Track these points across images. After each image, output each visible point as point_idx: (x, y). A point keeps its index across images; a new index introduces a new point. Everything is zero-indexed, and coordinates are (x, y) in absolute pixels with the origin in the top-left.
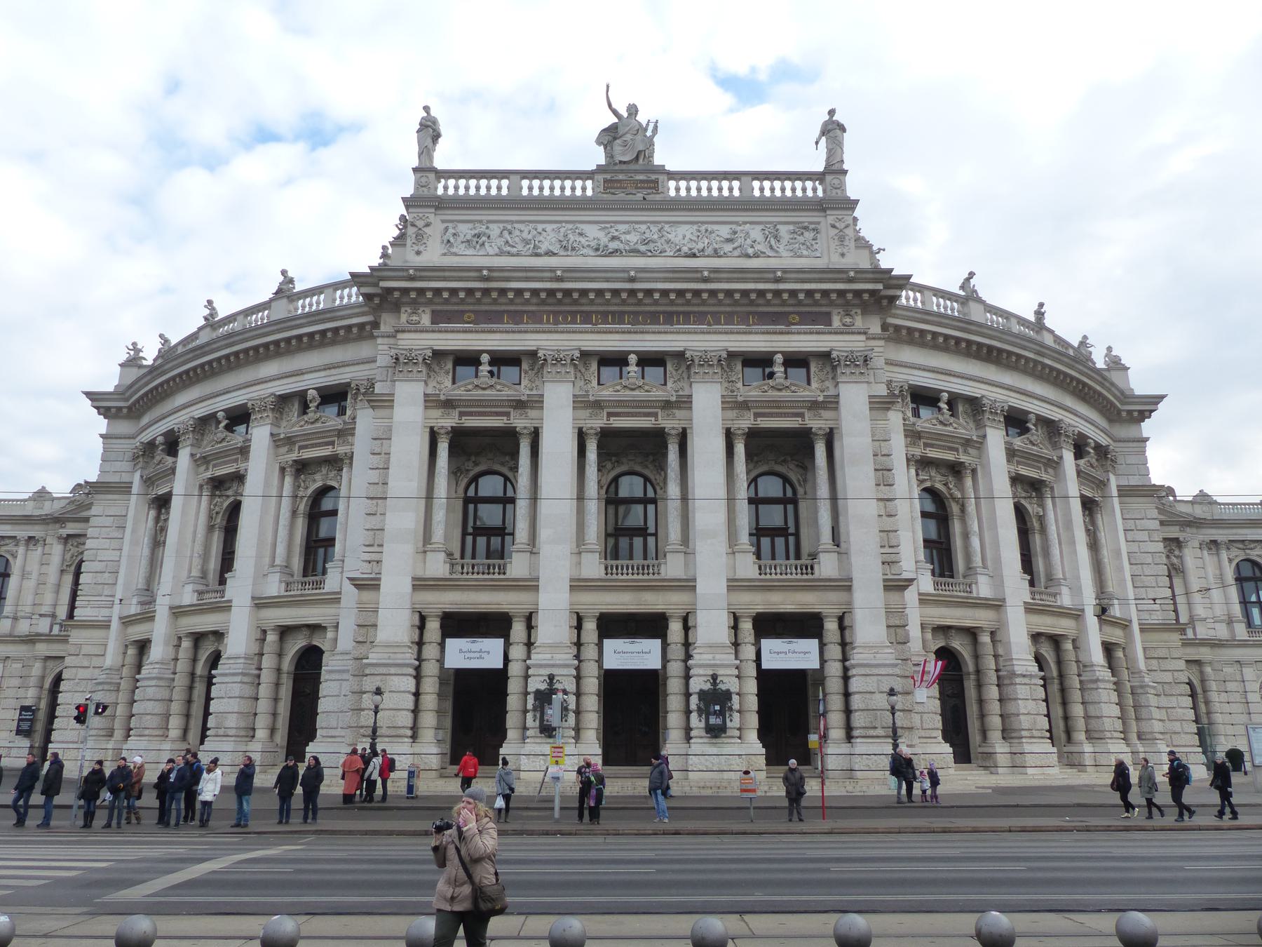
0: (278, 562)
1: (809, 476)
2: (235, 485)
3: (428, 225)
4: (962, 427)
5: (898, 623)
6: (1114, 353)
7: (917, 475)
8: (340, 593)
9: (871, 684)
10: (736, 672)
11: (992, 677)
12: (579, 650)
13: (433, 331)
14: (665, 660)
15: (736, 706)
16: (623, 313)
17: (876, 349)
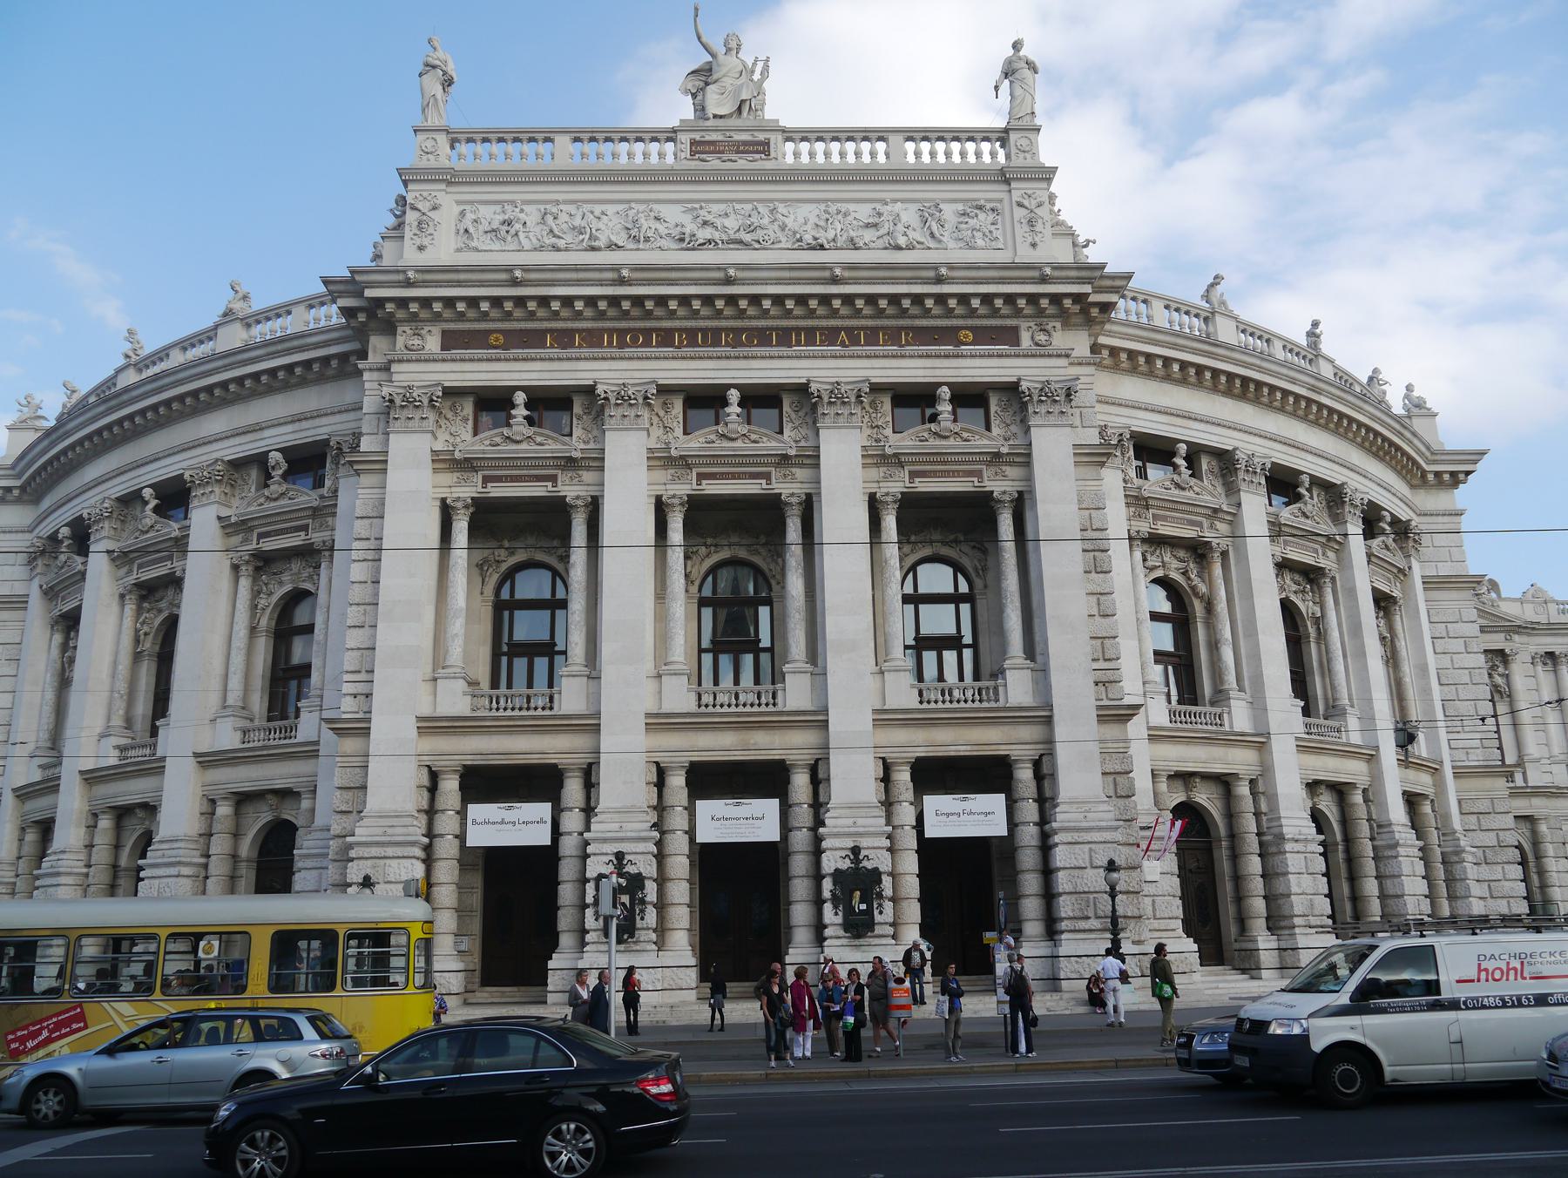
0: (230, 701)
1: (990, 563)
2: (170, 592)
3: (434, 208)
4: (1208, 492)
5: (1118, 768)
6: (1416, 394)
7: (1145, 560)
8: (317, 743)
9: (1080, 855)
10: (887, 843)
11: (1252, 843)
12: (660, 817)
13: (444, 360)
14: (786, 827)
15: (888, 892)
16: (717, 332)
17: (1083, 379)
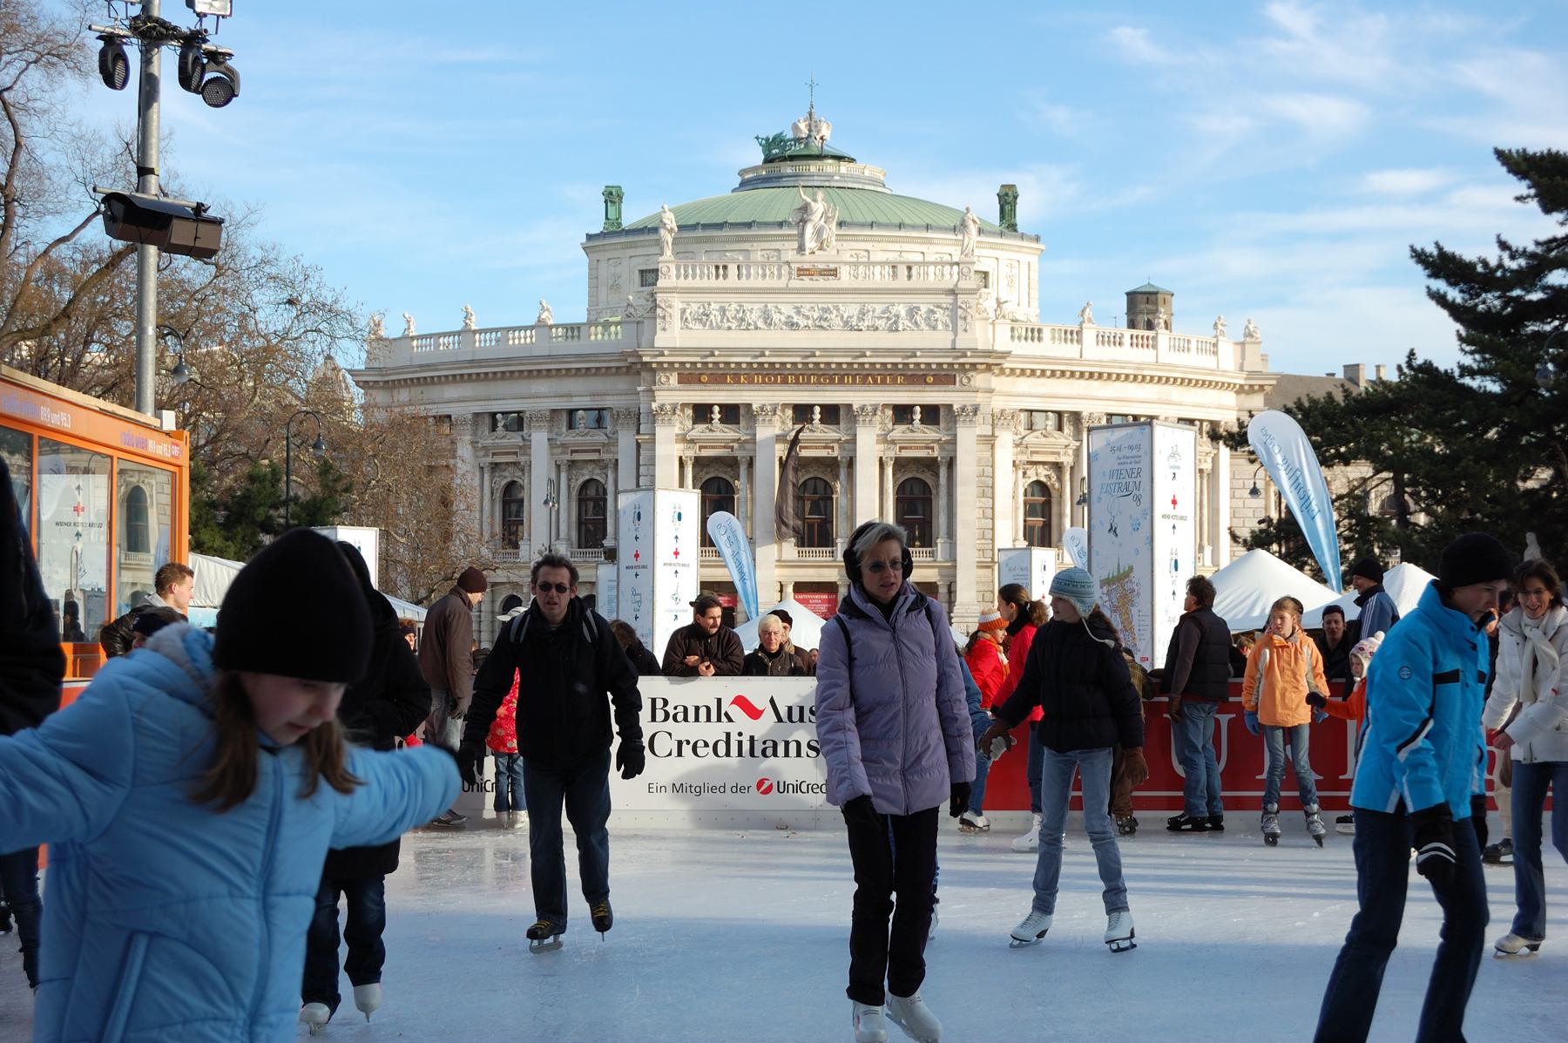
0: (562, 535)
2: (511, 469)
